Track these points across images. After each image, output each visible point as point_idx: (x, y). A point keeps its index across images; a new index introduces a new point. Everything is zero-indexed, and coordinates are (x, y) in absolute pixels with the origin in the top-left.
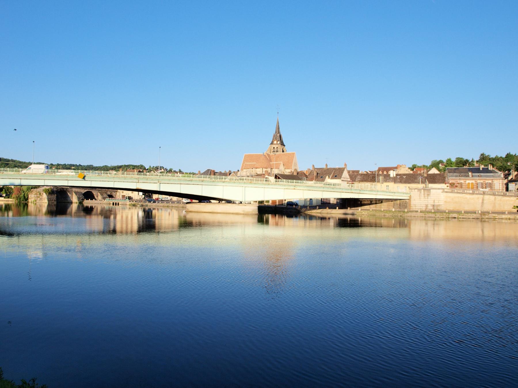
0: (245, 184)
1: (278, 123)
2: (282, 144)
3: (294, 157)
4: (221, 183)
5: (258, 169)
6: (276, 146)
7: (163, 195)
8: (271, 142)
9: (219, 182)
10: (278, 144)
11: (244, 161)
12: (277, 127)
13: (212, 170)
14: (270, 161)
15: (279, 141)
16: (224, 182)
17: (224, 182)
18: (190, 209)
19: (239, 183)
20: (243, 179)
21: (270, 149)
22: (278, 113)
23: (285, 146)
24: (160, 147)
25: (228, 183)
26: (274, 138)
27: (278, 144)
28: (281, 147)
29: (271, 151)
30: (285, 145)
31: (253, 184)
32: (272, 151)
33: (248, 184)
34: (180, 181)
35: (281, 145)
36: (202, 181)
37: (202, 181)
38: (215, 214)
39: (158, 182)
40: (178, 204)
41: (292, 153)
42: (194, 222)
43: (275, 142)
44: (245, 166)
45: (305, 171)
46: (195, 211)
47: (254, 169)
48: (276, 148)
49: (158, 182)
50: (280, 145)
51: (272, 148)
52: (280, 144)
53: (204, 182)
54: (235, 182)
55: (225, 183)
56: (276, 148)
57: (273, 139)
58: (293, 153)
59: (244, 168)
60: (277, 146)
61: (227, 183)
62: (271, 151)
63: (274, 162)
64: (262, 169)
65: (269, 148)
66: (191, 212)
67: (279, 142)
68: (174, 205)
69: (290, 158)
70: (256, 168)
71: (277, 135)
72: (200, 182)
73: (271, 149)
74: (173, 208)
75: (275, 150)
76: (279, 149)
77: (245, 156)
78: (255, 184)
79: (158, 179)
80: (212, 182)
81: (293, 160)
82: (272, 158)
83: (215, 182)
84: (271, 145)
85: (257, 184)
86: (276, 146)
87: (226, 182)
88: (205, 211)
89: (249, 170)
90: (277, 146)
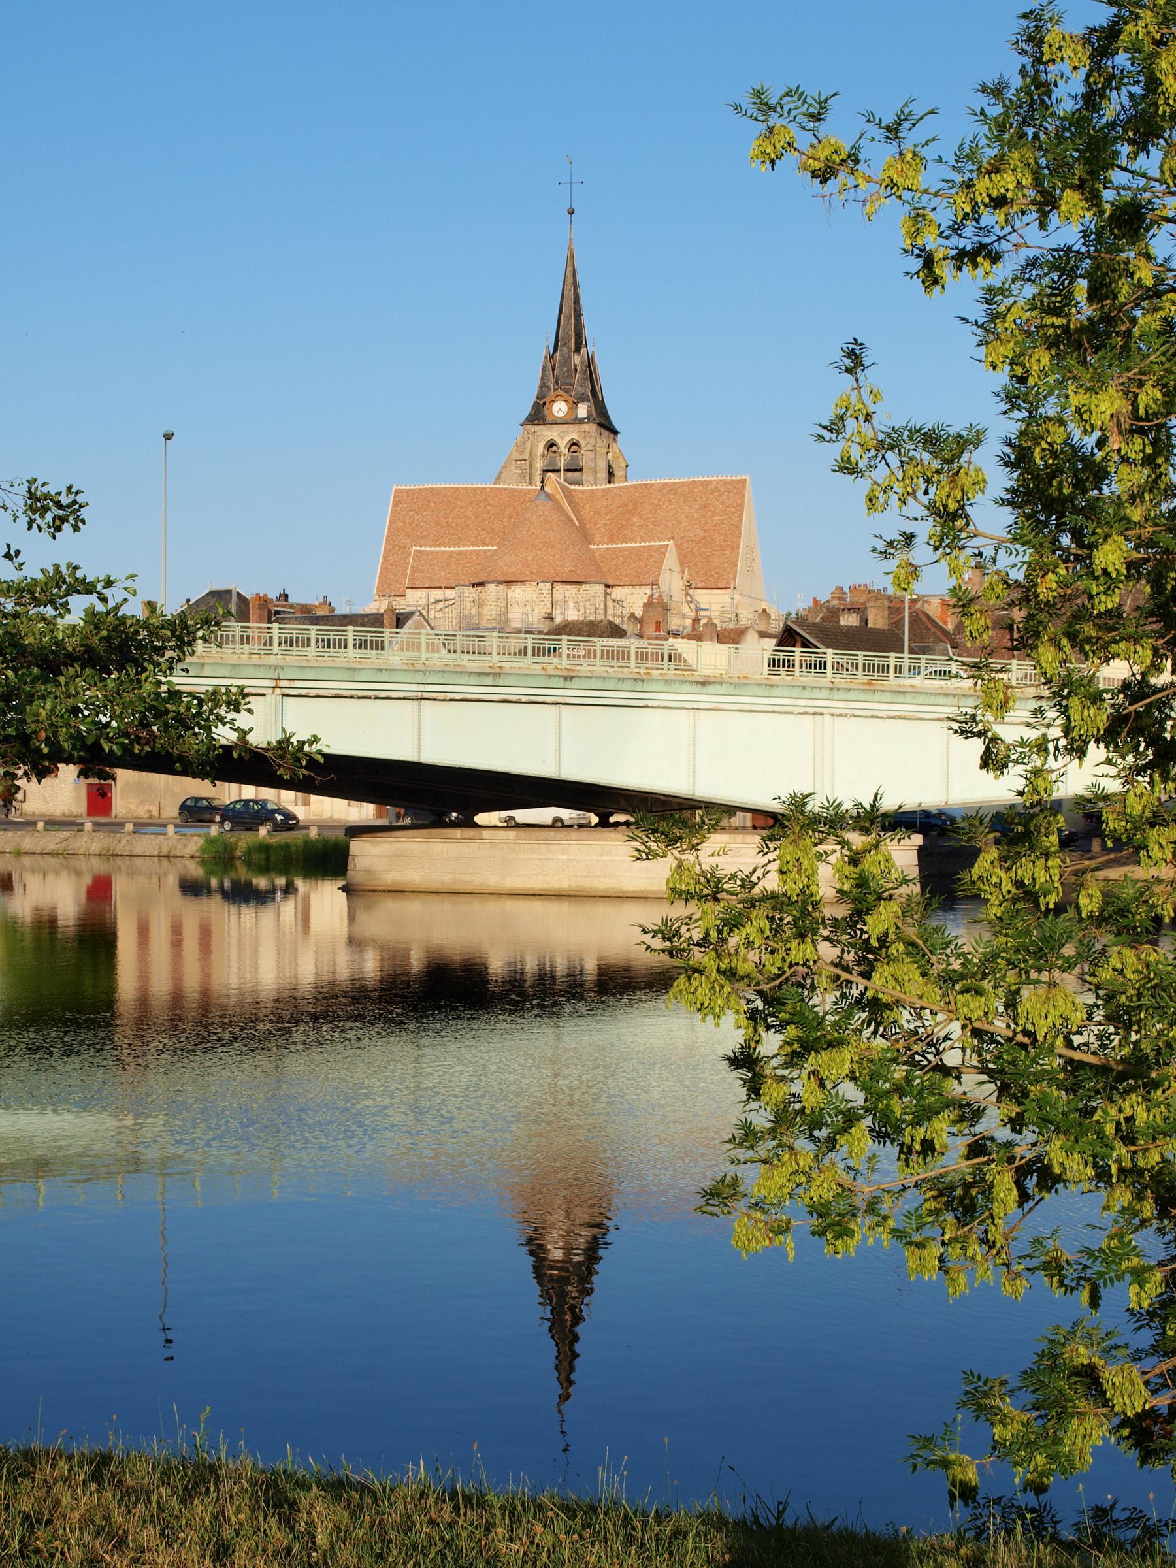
0: (836, 695)
1: (570, 280)
2: (607, 426)
3: (741, 506)
4: (686, 687)
5: (517, 592)
6: (562, 437)
7: (244, 786)
8: (527, 409)
9: (677, 688)
10: (581, 421)
11: (393, 532)
12: (568, 308)
13: (247, 595)
14: (586, 537)
15: (581, 399)
16: (703, 684)
17: (703, 684)
18: (392, 876)
19: (796, 692)
20: (624, 655)
21: (526, 455)
22: (571, 212)
23: (616, 433)
24: (168, 437)
25: (731, 690)
26: (551, 384)
27: (581, 421)
28: (599, 441)
29: (531, 467)
30: (618, 429)
31: (888, 697)
32: (539, 465)
33: (852, 695)
34: (419, 678)
35: (600, 425)
36: (565, 678)
37: (565, 678)
38: (602, 910)
39: (273, 683)
40: (65, 834)
41: (725, 483)
42: (497, 964)
43: (559, 408)
44: (414, 570)
45: (936, 602)
46: (434, 886)
47: (491, 587)
48: (563, 444)
49: (273, 683)
50: (592, 428)
51: (540, 449)
52: (589, 419)
53: (575, 683)
54: (772, 686)
55: (710, 689)
56: (563, 444)
57: (543, 385)
58: (731, 482)
59: (413, 579)
60: (573, 433)
61: (722, 689)
62: (531, 467)
63: (601, 543)
64: (548, 586)
65: (520, 447)
66: (399, 892)
67: (582, 411)
68: (27, 842)
69: (714, 514)
70: (509, 583)
71: (567, 361)
72: (554, 682)
73: (531, 454)
74: (27, 861)
75: (562, 463)
76: (585, 460)
77: (396, 503)
78: (900, 698)
79: (276, 667)
80: (628, 685)
81: (738, 527)
82: (587, 512)
83: (646, 687)
84: (532, 428)
85: (909, 698)
86: (562, 437)
87: (721, 684)
88: (494, 881)
89: (450, 594)
90: (575, 436)
